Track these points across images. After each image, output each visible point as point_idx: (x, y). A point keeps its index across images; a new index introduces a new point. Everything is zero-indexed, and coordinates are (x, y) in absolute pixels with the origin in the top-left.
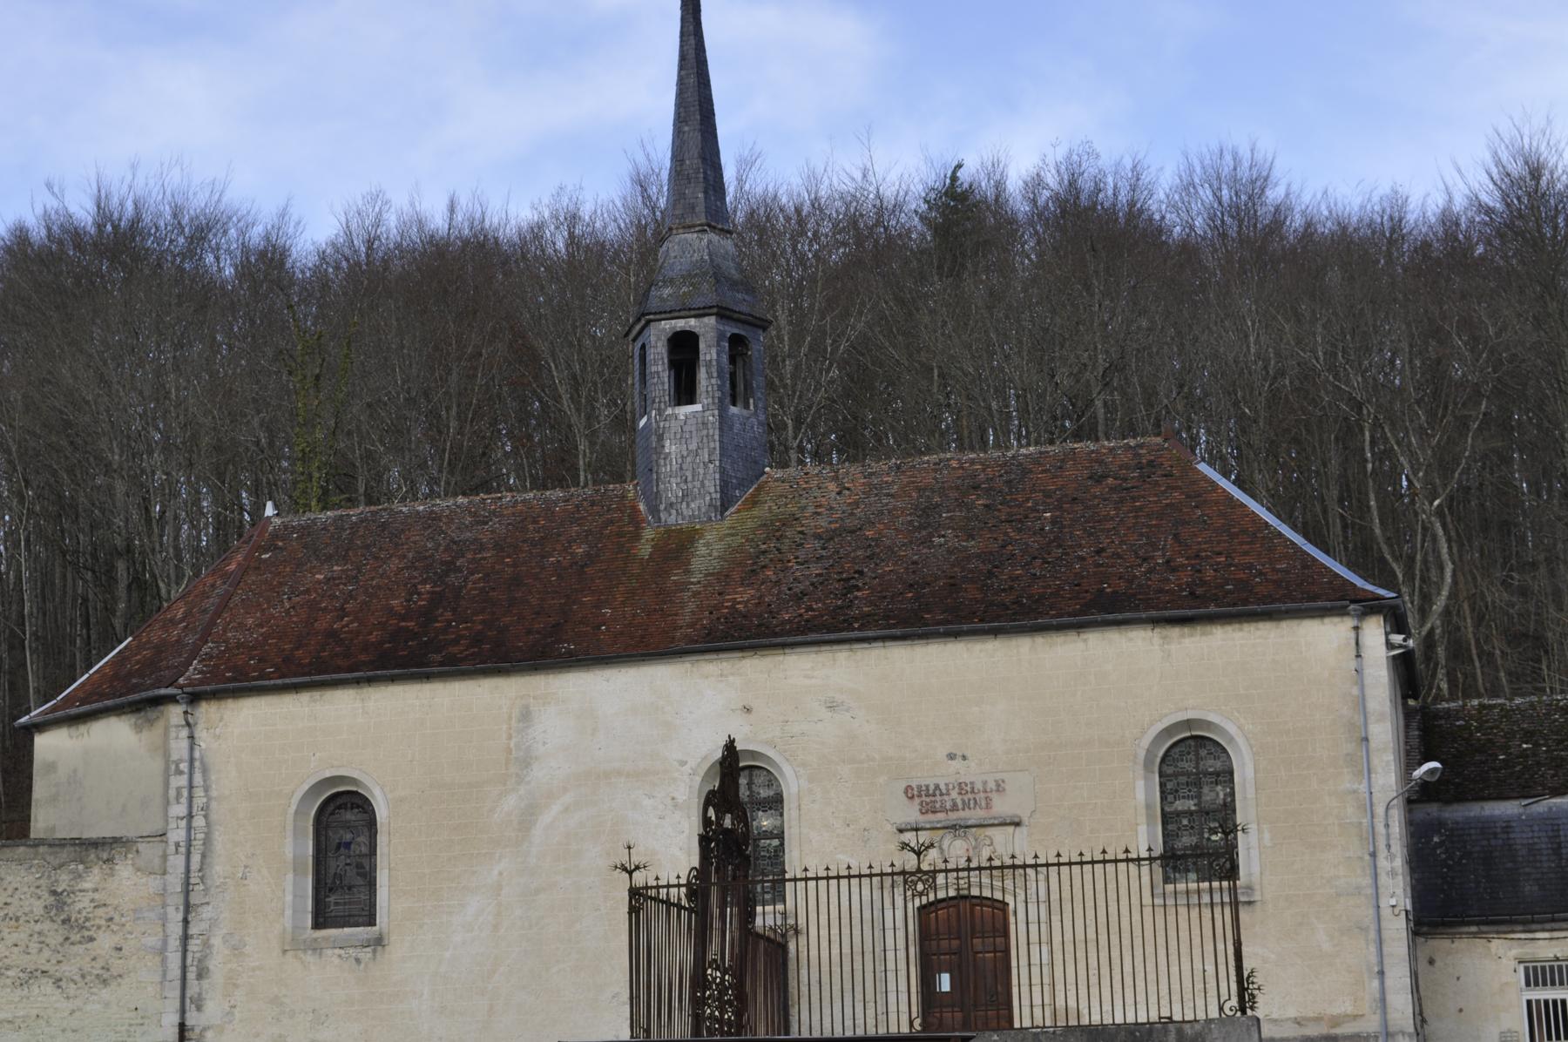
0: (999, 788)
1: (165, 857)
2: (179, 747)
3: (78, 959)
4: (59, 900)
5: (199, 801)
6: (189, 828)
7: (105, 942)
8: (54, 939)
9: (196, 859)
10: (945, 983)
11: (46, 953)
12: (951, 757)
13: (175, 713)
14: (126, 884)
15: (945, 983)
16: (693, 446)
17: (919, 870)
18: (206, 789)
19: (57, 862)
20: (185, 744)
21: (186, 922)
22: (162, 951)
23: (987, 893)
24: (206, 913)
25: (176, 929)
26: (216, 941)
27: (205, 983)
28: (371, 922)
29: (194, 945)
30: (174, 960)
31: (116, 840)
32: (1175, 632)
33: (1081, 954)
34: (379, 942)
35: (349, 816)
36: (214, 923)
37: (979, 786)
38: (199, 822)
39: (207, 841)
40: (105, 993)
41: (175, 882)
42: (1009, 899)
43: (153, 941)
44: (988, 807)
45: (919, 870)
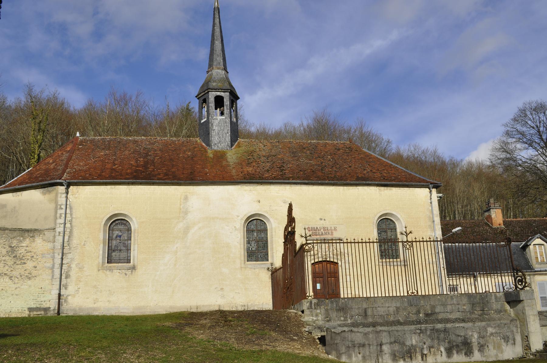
0: (335, 229)
1: (54, 237)
2: (62, 200)
3: (19, 270)
4: (12, 249)
5: (68, 218)
6: (65, 227)
7: (30, 265)
8: (10, 263)
9: (66, 238)
10: (318, 286)
11: (7, 267)
12: (321, 219)
13: (62, 189)
14: (39, 245)
15: (318, 286)
16: (222, 128)
17: (407, 241)
18: (71, 215)
19: (13, 236)
20: (64, 199)
21: (62, 259)
22: (52, 268)
23: (332, 260)
24: (70, 256)
25: (58, 261)
26: (73, 266)
27: (68, 280)
28: (128, 261)
29: (64, 267)
30: (57, 272)
31: (36, 230)
32: (382, 188)
33: (360, 279)
34: (134, 268)
35: (121, 227)
36: (72, 259)
37: (329, 228)
38: (68, 225)
39: (71, 232)
40: (29, 282)
41: (58, 245)
43: (49, 265)
44: (332, 234)
45: (407, 241)
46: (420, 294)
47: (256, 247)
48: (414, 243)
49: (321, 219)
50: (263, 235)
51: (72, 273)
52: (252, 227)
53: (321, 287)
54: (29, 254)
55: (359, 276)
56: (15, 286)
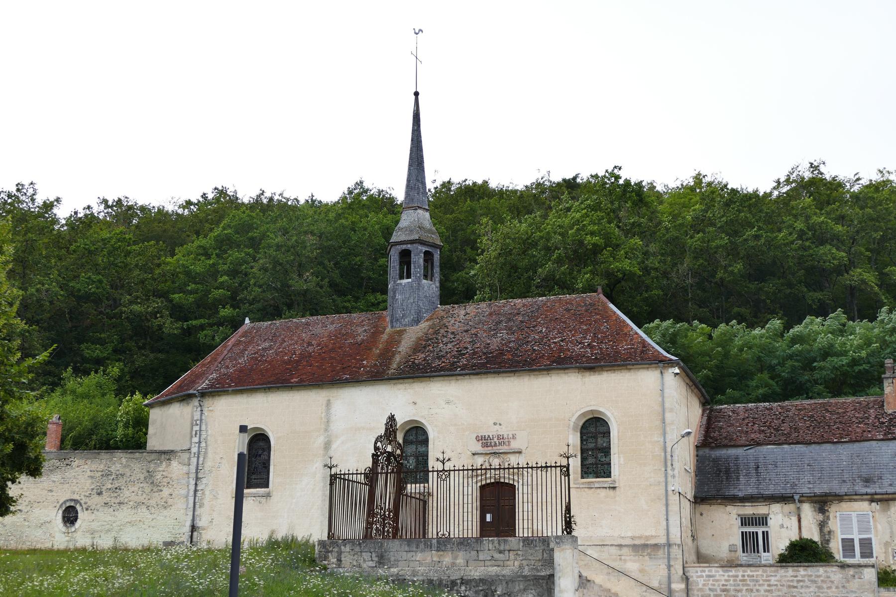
0: (514, 437)
1: (189, 459)
2: (197, 416)
3: (156, 499)
4: (150, 474)
5: (203, 437)
6: (199, 447)
7: (166, 492)
8: (147, 490)
9: (201, 459)
10: (489, 518)
11: (144, 496)
12: (495, 424)
13: (195, 402)
14: (176, 468)
15: (489, 518)
16: (407, 296)
17: (443, 470)
18: (207, 431)
19: (149, 460)
20: (199, 413)
21: (196, 484)
22: (187, 497)
23: (507, 481)
24: (204, 481)
25: (192, 488)
26: (207, 493)
27: (202, 509)
28: (267, 486)
29: (199, 494)
30: (191, 499)
31: (172, 451)
32: (587, 374)
33: (544, 507)
34: (268, 495)
35: (261, 444)
36: (206, 485)
37: (505, 436)
38: (203, 444)
39: (206, 453)
40: (165, 512)
41: (193, 468)
42: (516, 484)
43: (184, 492)
44: (509, 445)
45: (443, 470)
46: (452, 536)
47: (414, 464)
48: (452, 473)
49: (495, 424)
50: (422, 449)
51: (206, 502)
52: (411, 437)
53: (493, 518)
54: (165, 480)
55: (544, 504)
56: (150, 516)
